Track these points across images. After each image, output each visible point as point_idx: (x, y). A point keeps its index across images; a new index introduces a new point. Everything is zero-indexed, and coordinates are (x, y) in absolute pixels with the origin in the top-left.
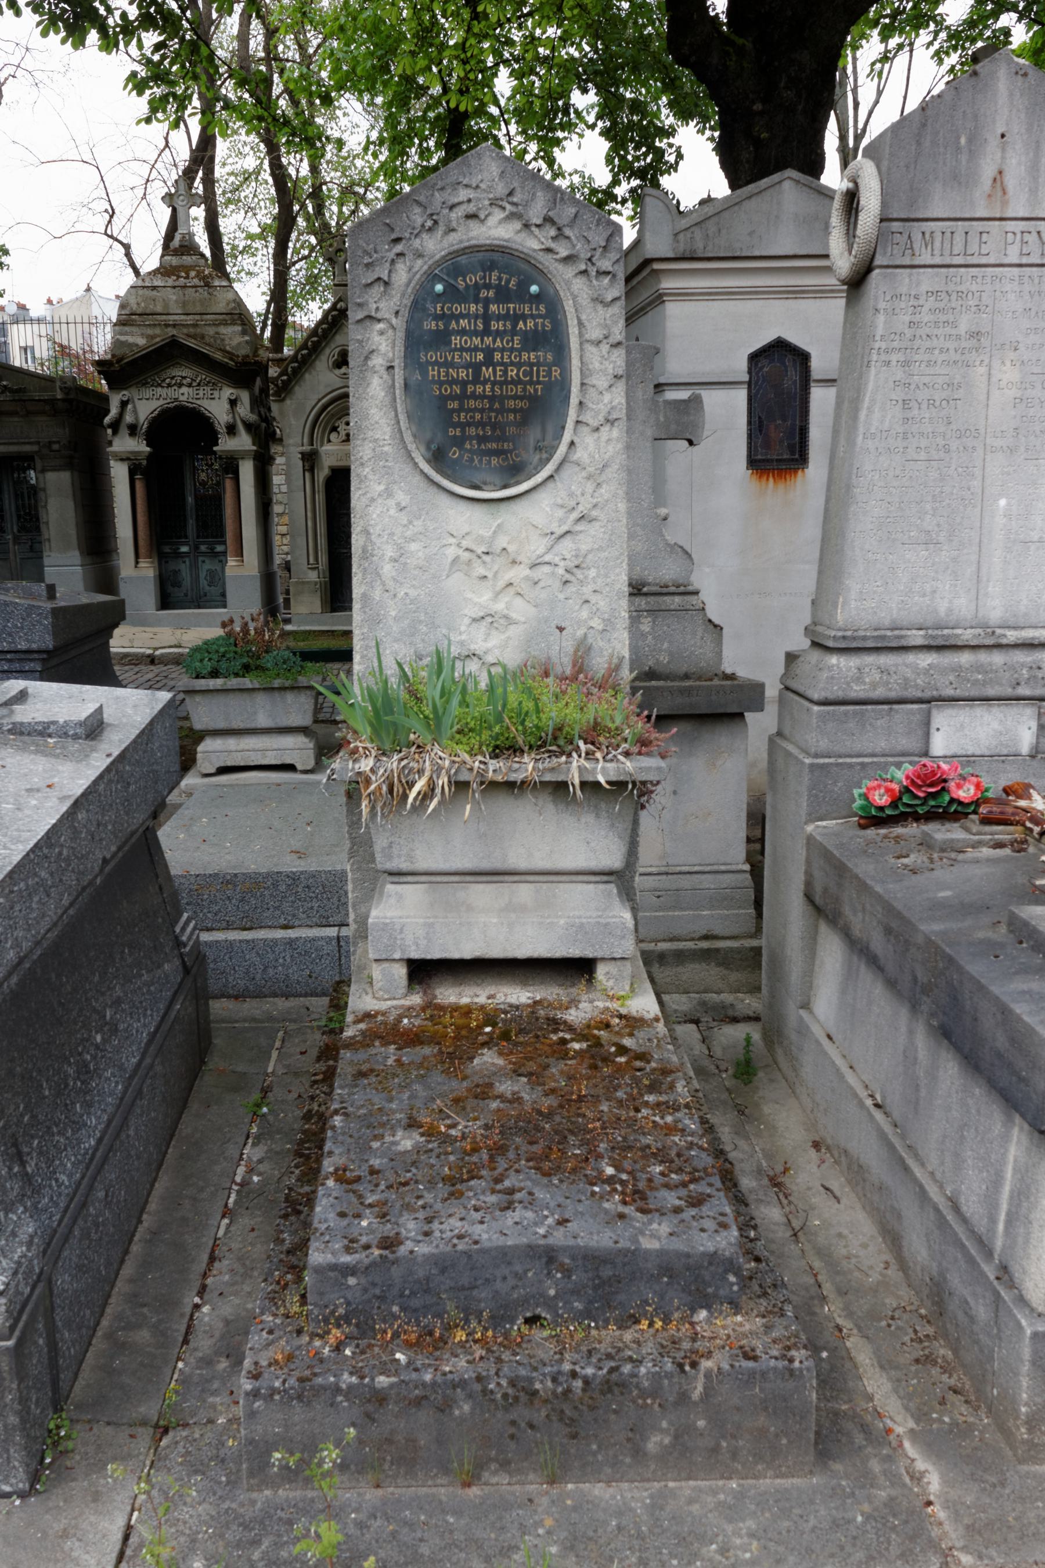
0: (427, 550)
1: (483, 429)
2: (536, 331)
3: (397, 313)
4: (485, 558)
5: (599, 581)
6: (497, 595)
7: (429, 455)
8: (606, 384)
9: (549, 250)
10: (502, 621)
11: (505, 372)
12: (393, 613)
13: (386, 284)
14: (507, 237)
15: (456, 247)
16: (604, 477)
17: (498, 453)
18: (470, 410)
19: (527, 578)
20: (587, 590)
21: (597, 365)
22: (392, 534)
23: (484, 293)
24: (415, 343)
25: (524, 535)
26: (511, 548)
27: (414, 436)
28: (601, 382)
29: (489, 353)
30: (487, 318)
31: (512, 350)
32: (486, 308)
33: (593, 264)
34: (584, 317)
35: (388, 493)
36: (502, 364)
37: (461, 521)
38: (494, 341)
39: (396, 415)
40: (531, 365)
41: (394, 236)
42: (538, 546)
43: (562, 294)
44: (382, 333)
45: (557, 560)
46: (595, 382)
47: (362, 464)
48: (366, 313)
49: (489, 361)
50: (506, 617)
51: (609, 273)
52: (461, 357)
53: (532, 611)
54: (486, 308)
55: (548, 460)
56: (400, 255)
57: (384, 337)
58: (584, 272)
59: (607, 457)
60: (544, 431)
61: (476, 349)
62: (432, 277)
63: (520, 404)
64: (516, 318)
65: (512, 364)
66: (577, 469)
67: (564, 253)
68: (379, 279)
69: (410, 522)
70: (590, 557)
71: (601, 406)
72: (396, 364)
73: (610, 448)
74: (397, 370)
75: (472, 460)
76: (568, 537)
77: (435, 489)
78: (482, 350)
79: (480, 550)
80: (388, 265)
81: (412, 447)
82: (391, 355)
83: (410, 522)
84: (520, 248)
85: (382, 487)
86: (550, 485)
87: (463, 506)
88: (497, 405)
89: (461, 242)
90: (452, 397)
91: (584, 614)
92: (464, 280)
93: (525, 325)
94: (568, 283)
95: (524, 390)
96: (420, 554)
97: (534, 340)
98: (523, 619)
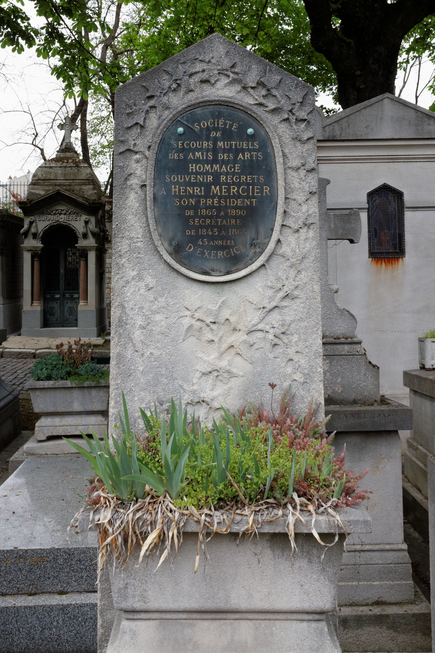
0: (168, 321)
1: (212, 231)
2: (251, 161)
3: (149, 147)
4: (212, 326)
5: (301, 344)
6: (222, 354)
7: (171, 249)
8: (304, 199)
9: (261, 105)
10: (225, 375)
11: (229, 190)
12: (141, 369)
13: (142, 127)
14: (230, 95)
15: (193, 102)
16: (303, 266)
17: (222, 248)
18: (202, 217)
19: (245, 342)
20: (291, 351)
21: (297, 185)
22: (141, 308)
23: (213, 134)
24: (161, 168)
25: (242, 309)
26: (233, 319)
27: (160, 235)
28: (300, 197)
29: (217, 175)
30: (215, 151)
31: (234, 174)
32: (215, 144)
33: (293, 114)
34: (286, 151)
35: (140, 277)
36: (227, 184)
37: (195, 298)
38: (221, 168)
39: (147, 221)
40: (248, 184)
41: (148, 94)
42: (253, 318)
43: (270, 135)
44: (138, 161)
45: (268, 328)
46: (295, 197)
47: (121, 256)
48: (126, 148)
49: (216, 182)
50: (228, 372)
51: (305, 120)
52: (196, 178)
53: (249, 367)
54: (215, 144)
55: (261, 253)
56: (151, 107)
57: (139, 165)
58: (287, 120)
59: (305, 251)
60: (257, 232)
61: (207, 173)
62: (175, 121)
63: (239, 212)
64: (237, 151)
65: (234, 184)
66: (283, 260)
67: (272, 106)
68: (137, 124)
69: (156, 299)
70: (293, 325)
71: (300, 214)
72: (147, 183)
73: (307, 245)
74: (148, 188)
75: (203, 253)
76: (276, 311)
77: (175, 275)
78: (212, 174)
79: (209, 320)
80: (143, 114)
81: (158, 243)
82: (144, 177)
83: (156, 299)
84: (240, 103)
85: (135, 273)
86: (262, 271)
87: (196, 287)
88: (222, 213)
89: (197, 98)
90: (189, 207)
91: (289, 370)
92: (199, 125)
93: (244, 156)
94: (275, 127)
95: (243, 202)
96: (163, 323)
97: (251, 167)
98: (241, 373)
